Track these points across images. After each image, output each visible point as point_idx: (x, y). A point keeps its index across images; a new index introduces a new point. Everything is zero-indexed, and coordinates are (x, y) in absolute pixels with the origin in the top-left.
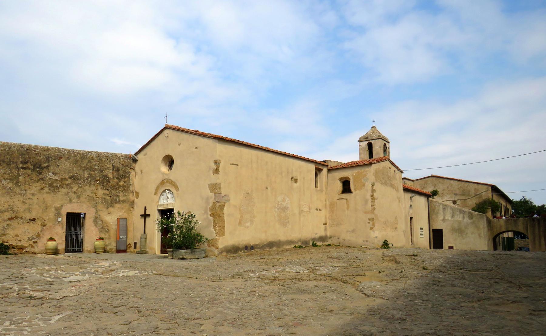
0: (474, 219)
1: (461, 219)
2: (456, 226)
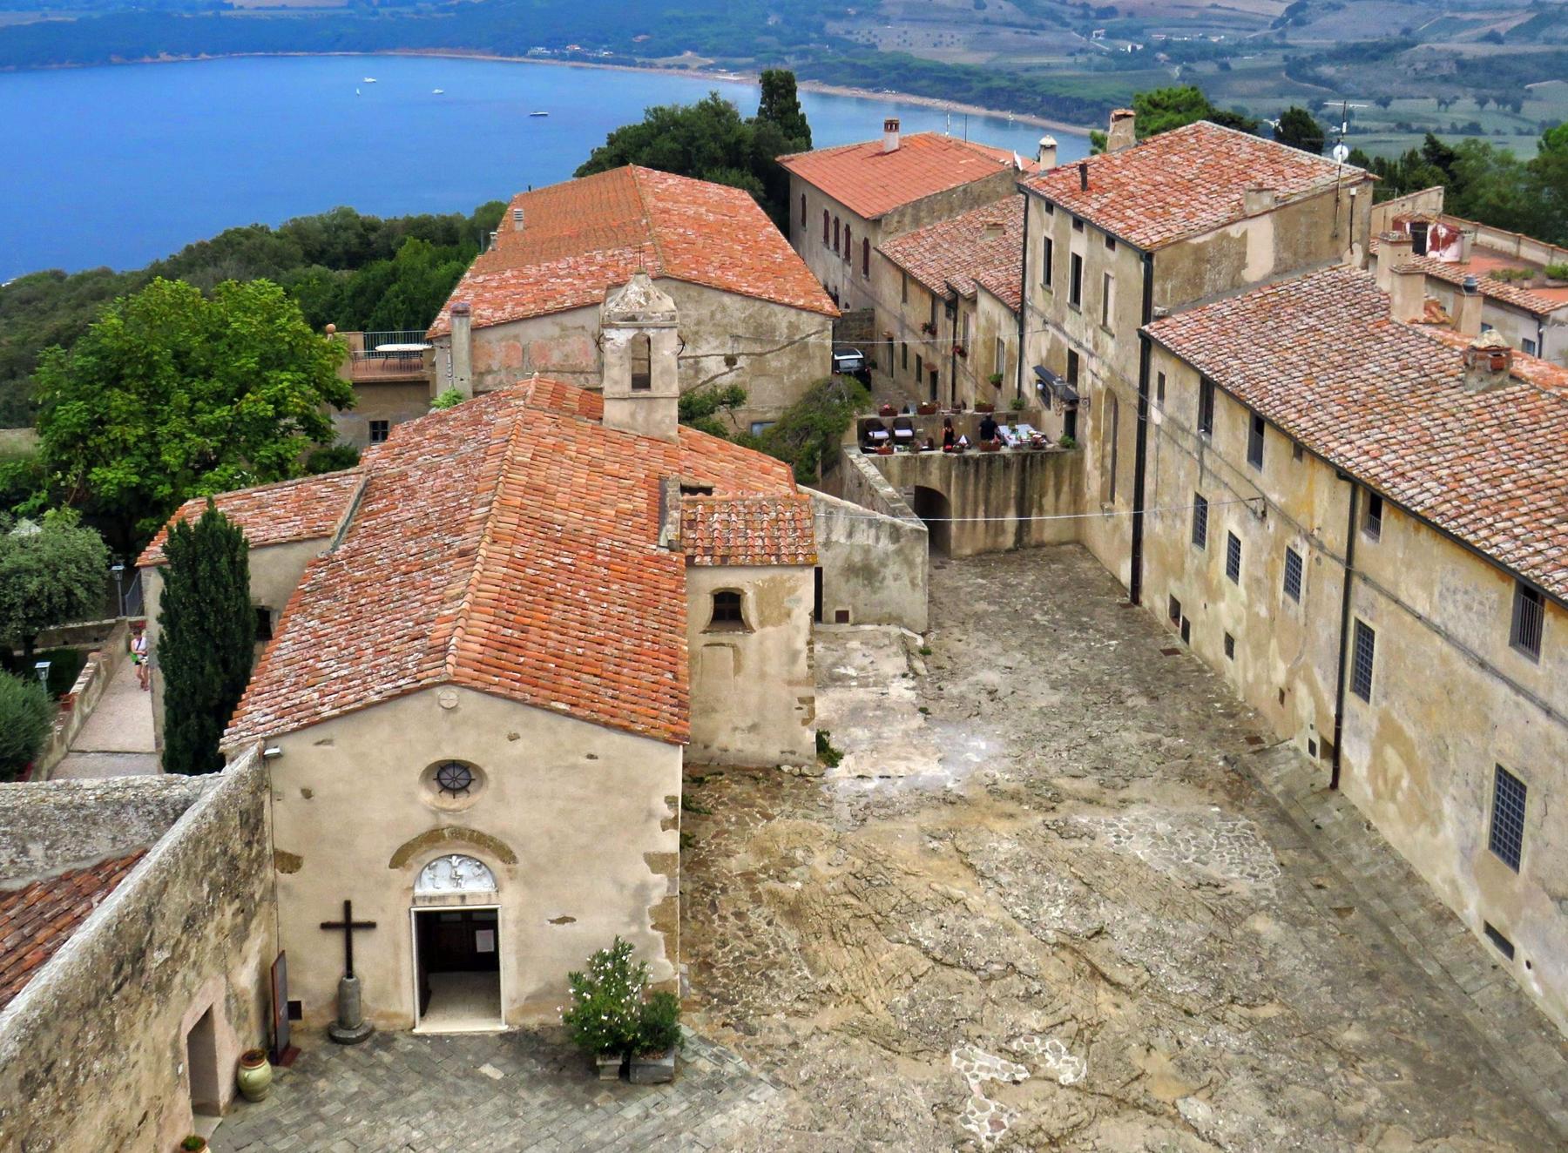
0: (903, 540)
1: (871, 542)
2: (857, 558)
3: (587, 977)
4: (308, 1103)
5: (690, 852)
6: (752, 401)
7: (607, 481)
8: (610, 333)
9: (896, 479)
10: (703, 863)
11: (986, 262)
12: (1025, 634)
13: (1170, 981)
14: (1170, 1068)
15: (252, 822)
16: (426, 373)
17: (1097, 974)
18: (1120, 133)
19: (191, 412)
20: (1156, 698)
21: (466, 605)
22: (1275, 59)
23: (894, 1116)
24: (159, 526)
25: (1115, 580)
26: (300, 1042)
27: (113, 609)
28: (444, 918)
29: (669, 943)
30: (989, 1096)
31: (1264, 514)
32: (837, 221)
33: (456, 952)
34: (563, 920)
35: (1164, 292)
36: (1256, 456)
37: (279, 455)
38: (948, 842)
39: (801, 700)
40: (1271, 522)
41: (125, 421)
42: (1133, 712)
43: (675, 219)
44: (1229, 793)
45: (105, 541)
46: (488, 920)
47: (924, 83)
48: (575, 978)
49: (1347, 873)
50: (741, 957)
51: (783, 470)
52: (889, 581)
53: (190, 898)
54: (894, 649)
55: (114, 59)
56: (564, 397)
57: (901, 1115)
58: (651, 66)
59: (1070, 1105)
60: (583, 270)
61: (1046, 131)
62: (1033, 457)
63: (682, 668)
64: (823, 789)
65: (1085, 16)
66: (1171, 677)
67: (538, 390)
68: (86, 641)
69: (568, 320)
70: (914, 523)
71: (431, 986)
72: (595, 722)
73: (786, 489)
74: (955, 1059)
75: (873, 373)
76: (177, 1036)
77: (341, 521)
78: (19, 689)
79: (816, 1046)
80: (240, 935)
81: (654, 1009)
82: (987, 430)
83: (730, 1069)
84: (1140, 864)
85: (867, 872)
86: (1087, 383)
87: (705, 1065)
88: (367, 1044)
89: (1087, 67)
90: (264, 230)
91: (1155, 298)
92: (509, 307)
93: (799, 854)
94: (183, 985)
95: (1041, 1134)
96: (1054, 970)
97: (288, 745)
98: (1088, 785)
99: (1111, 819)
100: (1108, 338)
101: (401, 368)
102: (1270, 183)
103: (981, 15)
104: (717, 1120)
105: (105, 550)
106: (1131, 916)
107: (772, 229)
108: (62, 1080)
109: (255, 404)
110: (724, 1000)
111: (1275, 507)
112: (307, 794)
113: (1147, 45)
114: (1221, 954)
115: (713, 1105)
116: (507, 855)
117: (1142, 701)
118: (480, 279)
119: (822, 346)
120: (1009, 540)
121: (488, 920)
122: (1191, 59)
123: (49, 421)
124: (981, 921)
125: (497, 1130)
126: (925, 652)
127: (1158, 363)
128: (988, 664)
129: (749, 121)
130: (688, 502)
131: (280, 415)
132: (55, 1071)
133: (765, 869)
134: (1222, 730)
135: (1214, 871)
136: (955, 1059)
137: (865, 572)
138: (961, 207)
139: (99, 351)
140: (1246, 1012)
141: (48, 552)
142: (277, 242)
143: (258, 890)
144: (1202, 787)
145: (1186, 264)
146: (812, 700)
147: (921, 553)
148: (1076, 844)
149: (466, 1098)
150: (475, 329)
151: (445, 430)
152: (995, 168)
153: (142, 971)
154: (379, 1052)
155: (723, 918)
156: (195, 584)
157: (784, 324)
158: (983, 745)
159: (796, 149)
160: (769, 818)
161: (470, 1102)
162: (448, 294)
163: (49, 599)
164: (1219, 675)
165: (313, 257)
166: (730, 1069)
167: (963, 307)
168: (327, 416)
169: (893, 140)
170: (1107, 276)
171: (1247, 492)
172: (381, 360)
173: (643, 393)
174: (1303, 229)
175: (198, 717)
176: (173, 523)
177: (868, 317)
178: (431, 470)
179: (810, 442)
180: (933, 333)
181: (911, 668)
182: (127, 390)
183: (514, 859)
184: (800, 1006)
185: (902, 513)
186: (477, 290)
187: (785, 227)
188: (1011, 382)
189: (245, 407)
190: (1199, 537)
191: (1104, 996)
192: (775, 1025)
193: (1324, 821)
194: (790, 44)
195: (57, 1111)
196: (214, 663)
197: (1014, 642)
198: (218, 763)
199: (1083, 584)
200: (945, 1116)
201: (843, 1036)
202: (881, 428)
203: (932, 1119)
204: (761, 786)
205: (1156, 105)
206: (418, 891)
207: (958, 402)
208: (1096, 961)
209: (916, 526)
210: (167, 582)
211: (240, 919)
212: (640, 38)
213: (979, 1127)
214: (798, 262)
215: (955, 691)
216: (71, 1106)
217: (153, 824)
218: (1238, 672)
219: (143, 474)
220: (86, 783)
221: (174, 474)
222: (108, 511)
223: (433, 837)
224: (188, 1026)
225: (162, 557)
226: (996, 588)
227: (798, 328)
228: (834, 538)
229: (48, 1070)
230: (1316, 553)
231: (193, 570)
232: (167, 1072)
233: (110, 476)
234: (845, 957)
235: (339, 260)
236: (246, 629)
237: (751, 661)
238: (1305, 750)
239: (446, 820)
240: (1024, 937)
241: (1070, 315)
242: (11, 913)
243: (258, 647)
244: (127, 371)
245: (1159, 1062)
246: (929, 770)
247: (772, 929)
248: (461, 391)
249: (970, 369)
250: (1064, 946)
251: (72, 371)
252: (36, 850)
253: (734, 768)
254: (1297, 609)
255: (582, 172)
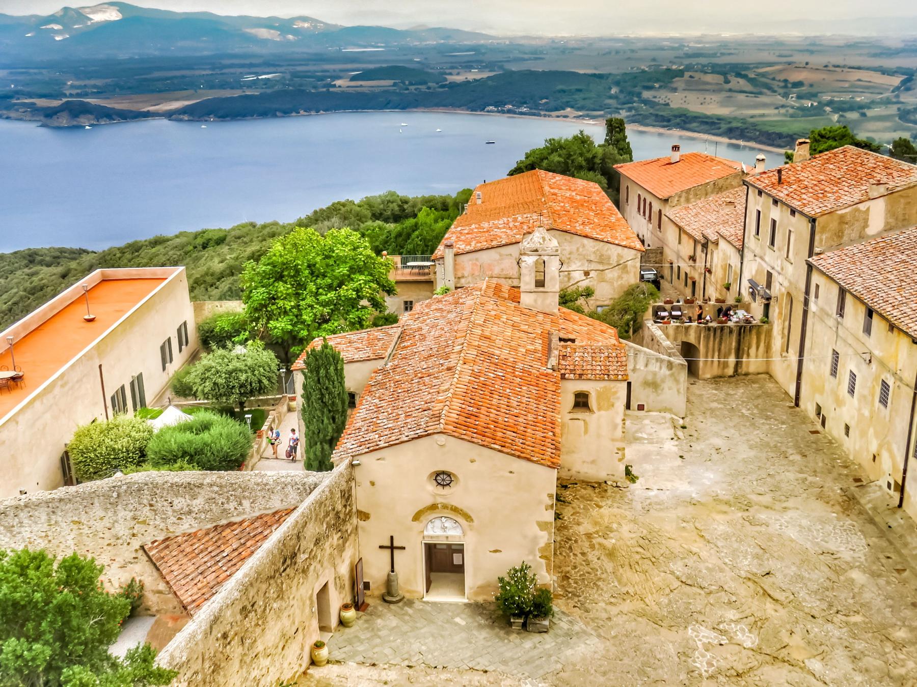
1: (657, 369)
2: (650, 378)
3: (507, 579)
4: (373, 629)
5: (559, 522)
6: (598, 294)
7: (523, 335)
8: (524, 258)
9: (672, 337)
10: (566, 528)
11: (725, 222)
12: (736, 420)
13: (805, 601)
14: (802, 644)
15: (347, 496)
16: (432, 277)
17: (766, 593)
18: (801, 152)
19: (316, 294)
20: (806, 456)
21: (450, 395)
22: (893, 110)
23: (658, 657)
24: (302, 351)
25: (786, 393)
26: (368, 601)
27: (280, 390)
28: (438, 547)
29: (548, 565)
30: (707, 650)
31: (870, 361)
32: (645, 200)
33: (443, 562)
34: (496, 551)
35: (821, 240)
36: (868, 330)
37: (359, 318)
38: (691, 524)
39: (619, 449)
40: (874, 365)
41: (285, 298)
42: (793, 463)
43: (559, 198)
44: (842, 507)
45: (277, 357)
46: (460, 550)
47: (695, 125)
48: (501, 580)
49: (905, 551)
50: (583, 575)
51: (612, 331)
52: (666, 390)
53: (318, 531)
54: (667, 425)
55: (278, 114)
56: (501, 291)
57: (662, 656)
58: (549, 116)
59: (749, 658)
60: (511, 225)
61: (760, 150)
62: (745, 329)
63: (557, 430)
64: (628, 494)
65: (785, 87)
66: (814, 445)
67: (488, 287)
68: (269, 405)
69: (503, 250)
70: (680, 360)
71: (432, 578)
72: (513, 455)
73: (613, 341)
74: (690, 631)
75: (662, 281)
76: (312, 594)
77: (389, 351)
78: (238, 427)
79: (620, 620)
80: (341, 549)
81: (540, 597)
82: (723, 312)
83: (576, 628)
84: (792, 540)
85: (649, 537)
86: (777, 290)
87: (564, 625)
88: (400, 604)
89: (785, 115)
90: (352, 203)
91: (816, 243)
92: (473, 244)
93: (615, 526)
94: (314, 570)
95: (733, 671)
96: (744, 591)
97: (363, 460)
98: (767, 499)
99: (778, 517)
100: (789, 265)
101: (419, 274)
102: (884, 180)
103: (727, 86)
104: (569, 652)
105: (276, 361)
106: (786, 567)
107: (610, 204)
108: (259, 611)
109: (347, 291)
110: (574, 595)
111: (876, 358)
112: (373, 484)
113: (819, 103)
114: (833, 588)
115: (568, 645)
116: (468, 517)
117: (798, 457)
118: (459, 229)
119: (635, 267)
120: (730, 371)
121: (460, 550)
122: (844, 110)
123: (249, 297)
124: (707, 564)
125: (462, 649)
126: (684, 427)
127: (816, 278)
128: (715, 433)
129: (599, 146)
130: (563, 346)
131: (360, 297)
132: (256, 606)
133: (597, 532)
134: (840, 474)
135: (832, 547)
136: (690, 631)
137: (653, 385)
138: (712, 193)
139: (272, 263)
140: (844, 618)
141: (250, 362)
142: (358, 209)
143: (349, 527)
144: (828, 503)
145: (834, 225)
146: (624, 449)
147: (683, 375)
148: (758, 528)
149: (447, 633)
150: (456, 255)
151: (441, 306)
152: (731, 171)
153: (295, 563)
154: (406, 608)
155: (575, 555)
156: (319, 380)
157: (615, 254)
158: (712, 476)
159: (624, 161)
160: (600, 507)
161: (450, 635)
162: (443, 237)
163: (251, 385)
164: (841, 445)
165: (376, 216)
166: (576, 628)
167: (710, 246)
168: (383, 298)
169: (676, 156)
170: (790, 231)
171: (861, 349)
172: (409, 270)
173: (541, 289)
174: (902, 206)
175: (321, 444)
176: (309, 349)
177: (660, 252)
178: (434, 326)
179: (627, 317)
180: (694, 261)
181: (676, 435)
182: (286, 283)
183: (472, 520)
184: (612, 600)
185: (675, 355)
186: (458, 234)
187: (617, 203)
188: (735, 288)
189: (342, 292)
190: (834, 372)
191: (769, 605)
192: (600, 608)
193: (893, 524)
194: (624, 104)
195: (257, 625)
196: (328, 419)
197: (731, 424)
198: (331, 467)
199: (768, 395)
200: (683, 658)
201: (633, 616)
202: (665, 310)
203: (677, 659)
204: (597, 491)
205: (822, 136)
206: (426, 533)
207: (706, 297)
208: (766, 588)
209: (681, 362)
210: (306, 378)
211: (341, 541)
212: (544, 101)
213: (701, 665)
214: (623, 222)
215: (698, 448)
216: (263, 622)
217: (300, 494)
218: (852, 446)
219: (294, 325)
220: (269, 473)
221: (309, 325)
222: (277, 343)
223: (433, 507)
224: (317, 590)
225: (303, 366)
226: (722, 395)
227: (622, 257)
228: (638, 367)
229: (253, 606)
230: (898, 383)
231: (318, 373)
232: (307, 610)
233: (278, 325)
234: (636, 578)
235: (388, 218)
236: (343, 402)
237: (592, 427)
238: (885, 486)
239: (439, 500)
240: (729, 574)
241: (768, 251)
242: (235, 532)
243: (349, 412)
244: (286, 273)
245: (796, 640)
246: (684, 488)
247: (599, 561)
248: (448, 286)
249: (713, 280)
250: (749, 579)
251: (258, 273)
252: (246, 503)
253: (583, 481)
254: (885, 412)
255: (511, 174)
